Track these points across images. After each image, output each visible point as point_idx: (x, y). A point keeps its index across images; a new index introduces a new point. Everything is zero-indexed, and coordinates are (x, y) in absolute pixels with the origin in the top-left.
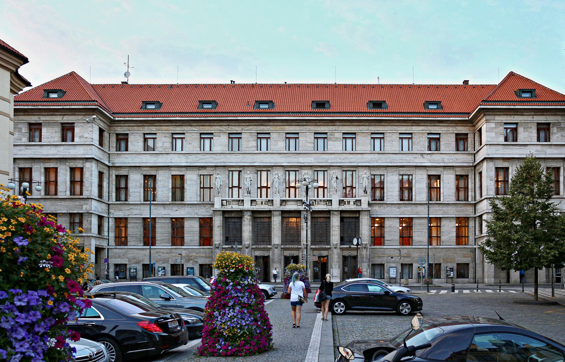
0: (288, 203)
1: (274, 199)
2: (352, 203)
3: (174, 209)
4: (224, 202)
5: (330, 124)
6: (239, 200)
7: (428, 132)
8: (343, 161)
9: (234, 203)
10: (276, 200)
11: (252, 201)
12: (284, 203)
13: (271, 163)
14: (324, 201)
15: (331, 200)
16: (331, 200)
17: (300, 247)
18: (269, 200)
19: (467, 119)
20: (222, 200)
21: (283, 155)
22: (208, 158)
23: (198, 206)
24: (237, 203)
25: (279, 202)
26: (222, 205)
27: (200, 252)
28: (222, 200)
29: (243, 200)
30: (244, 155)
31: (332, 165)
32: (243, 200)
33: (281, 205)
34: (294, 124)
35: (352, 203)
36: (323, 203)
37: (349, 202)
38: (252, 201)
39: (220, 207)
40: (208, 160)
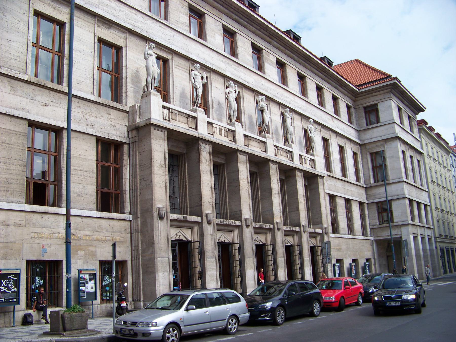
2: (308, 162)
3: (38, 98)
5: (268, 39)
7: (332, 92)
8: (281, 97)
13: (212, 65)
17: (272, 226)
19: (357, 90)
21: (222, 58)
22: (114, 9)
23: (93, 106)
24: (185, 120)
27: (100, 228)
30: (173, 33)
31: (274, 98)
34: (234, 17)
35: (308, 162)
36: (284, 154)
39: (162, 119)
40: (115, 13)
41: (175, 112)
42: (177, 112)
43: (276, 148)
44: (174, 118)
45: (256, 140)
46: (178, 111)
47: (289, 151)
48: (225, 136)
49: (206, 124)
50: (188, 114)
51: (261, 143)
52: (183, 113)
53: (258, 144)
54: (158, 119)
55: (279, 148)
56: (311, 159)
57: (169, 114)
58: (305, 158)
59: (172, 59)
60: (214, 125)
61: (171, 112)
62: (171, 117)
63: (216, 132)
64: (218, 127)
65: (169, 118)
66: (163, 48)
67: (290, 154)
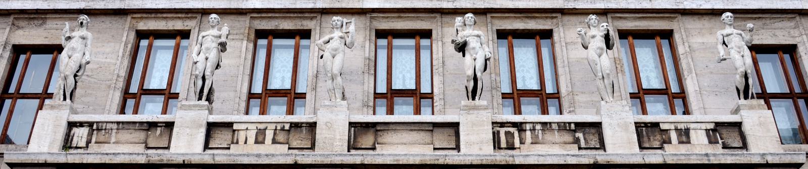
0: (388, 137)
1: (322, 118)
2: (699, 138)
4: (80, 134)
6: (152, 125)
9: (125, 135)
10: (329, 125)
11: (211, 127)
12: (367, 140)
14: (564, 127)
15: (597, 126)
16: (597, 126)
18: (296, 126)
20: (71, 125)
24: (141, 135)
25: (342, 134)
26: (67, 144)
28: (71, 125)
29: (170, 125)
32: (170, 125)
33: (352, 146)
36: (557, 137)
37: (685, 135)
38: (211, 127)
41: (109, 126)
42: (115, 126)
43: (512, 130)
44: (102, 139)
45: (409, 128)
46: (118, 123)
47: (580, 126)
48: (274, 141)
49: (203, 131)
50: (148, 123)
51: (436, 130)
52: (134, 123)
53: (429, 134)
54: (45, 149)
55: (528, 127)
56: (718, 124)
57: (90, 134)
58: (680, 126)
59: (194, 28)
60: (235, 127)
61: (98, 129)
62: (94, 140)
63: (242, 140)
64: (250, 126)
65: (88, 142)
66: (169, 15)
67: (593, 130)
